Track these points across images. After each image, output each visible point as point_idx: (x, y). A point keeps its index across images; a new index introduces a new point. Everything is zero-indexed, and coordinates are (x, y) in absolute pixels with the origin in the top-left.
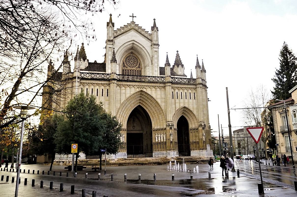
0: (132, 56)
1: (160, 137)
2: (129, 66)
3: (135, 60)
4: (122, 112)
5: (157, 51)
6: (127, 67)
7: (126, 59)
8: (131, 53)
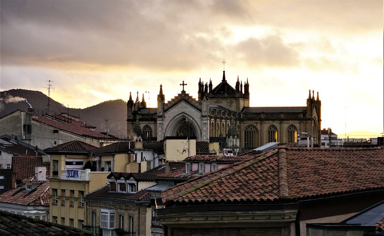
5: (206, 123)
7: (180, 129)
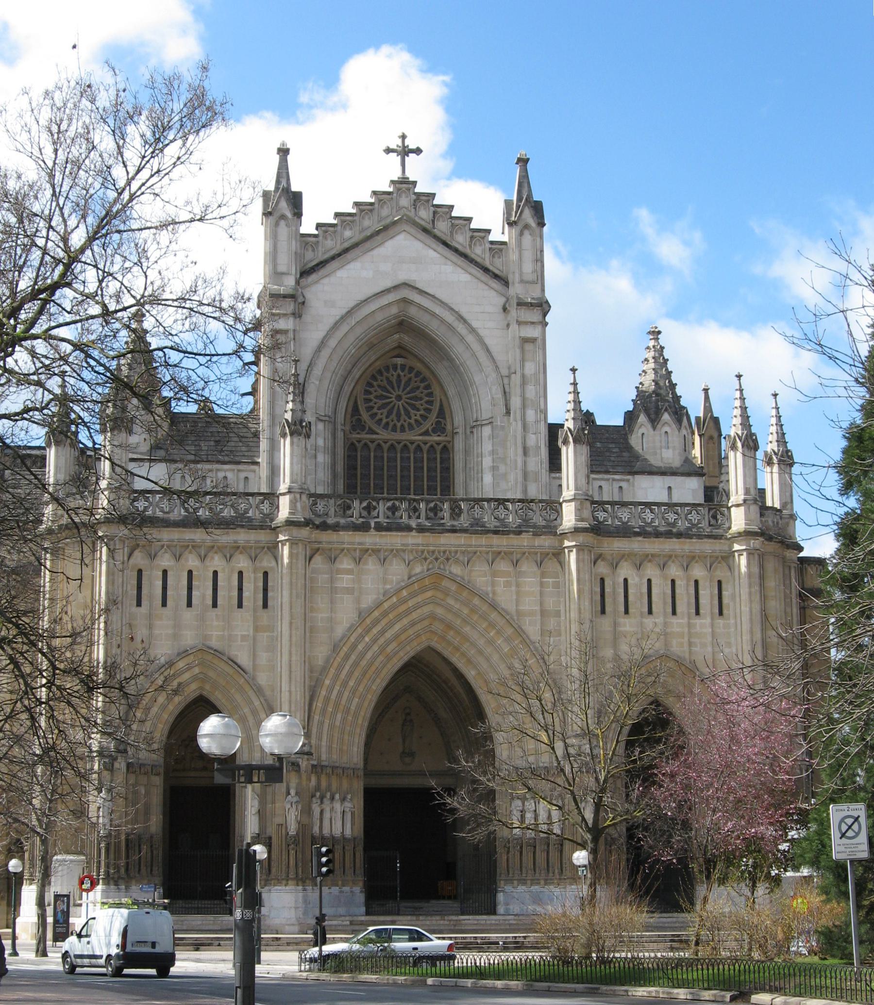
0: (403, 367)
1: (535, 811)
2: (384, 421)
3: (418, 388)
4: (337, 688)
5: (533, 340)
6: (372, 432)
7: (370, 385)
8: (396, 352)
